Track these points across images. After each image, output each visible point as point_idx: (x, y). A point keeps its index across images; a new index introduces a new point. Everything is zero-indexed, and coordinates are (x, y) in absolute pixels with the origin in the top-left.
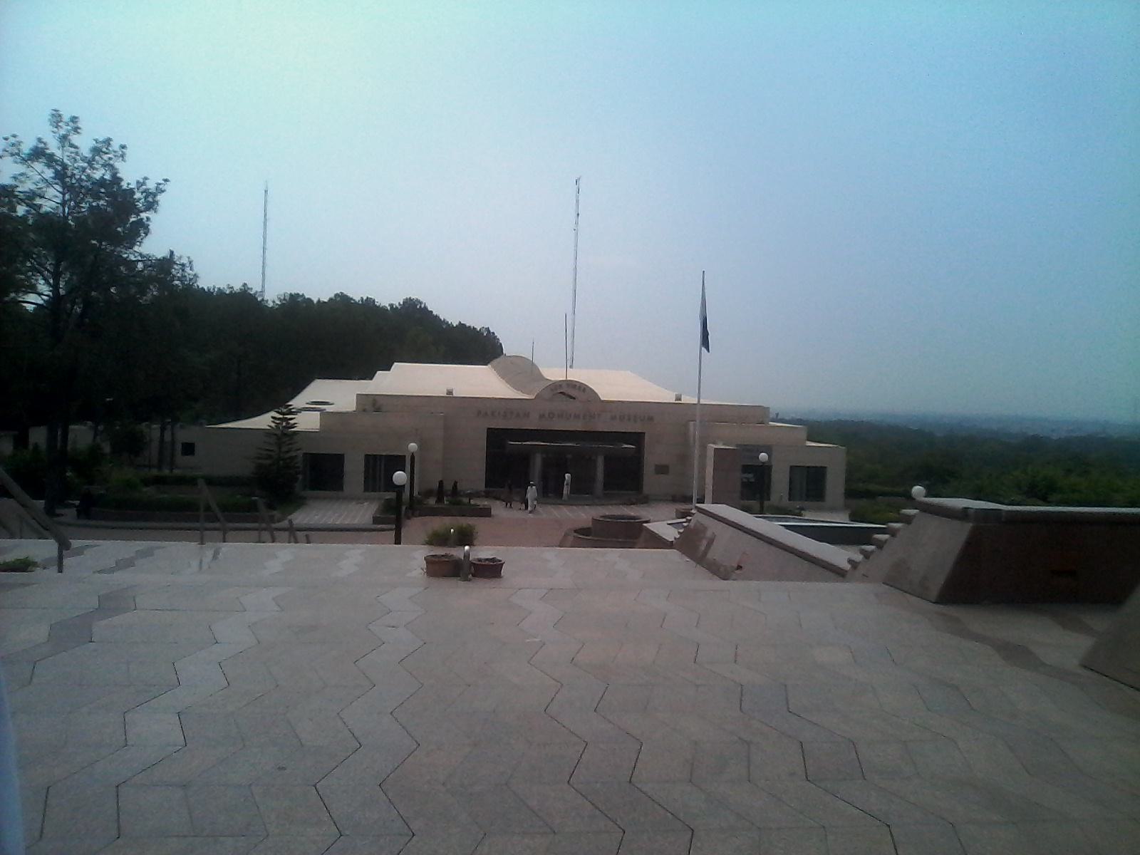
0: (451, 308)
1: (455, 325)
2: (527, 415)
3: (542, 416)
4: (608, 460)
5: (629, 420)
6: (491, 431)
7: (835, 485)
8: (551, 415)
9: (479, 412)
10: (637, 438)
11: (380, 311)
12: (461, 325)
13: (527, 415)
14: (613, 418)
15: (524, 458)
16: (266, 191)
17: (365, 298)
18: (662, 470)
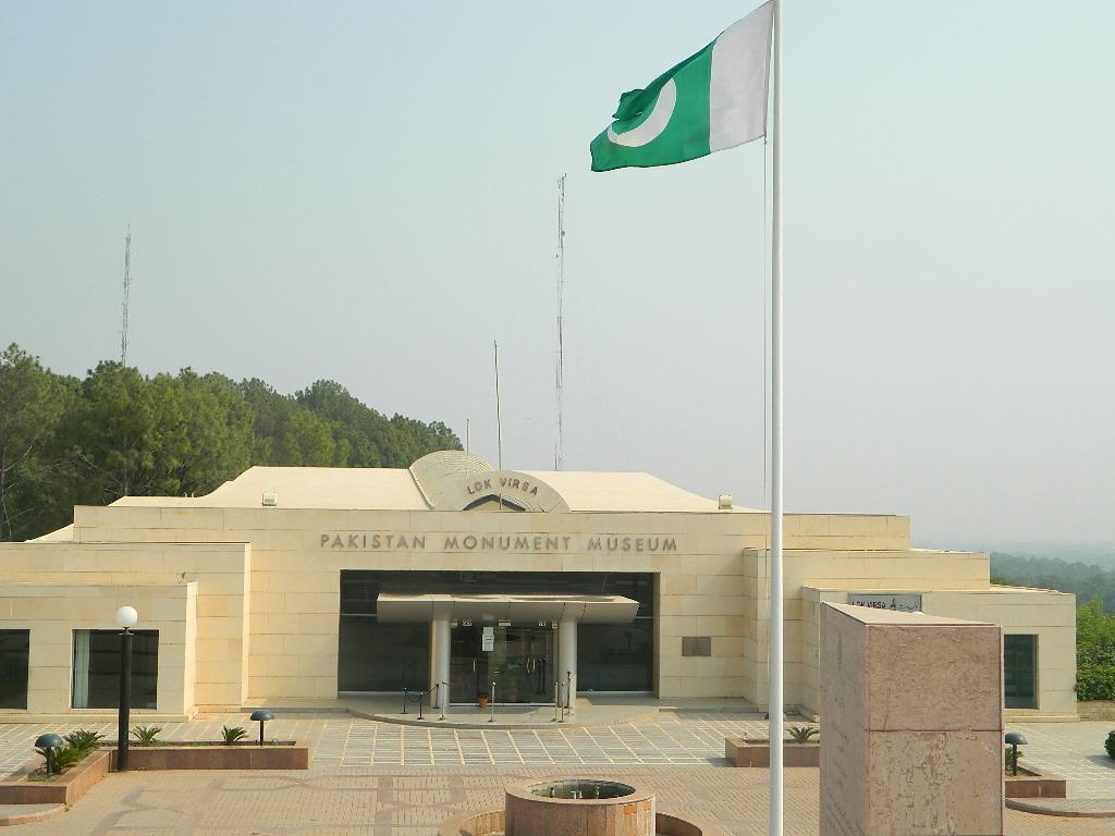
0: (383, 397)
1: (389, 419)
2: (419, 543)
3: (451, 543)
4: (589, 632)
6: (345, 575)
7: (1057, 668)
8: (470, 543)
9: (324, 539)
10: (643, 586)
12: (398, 419)
14: (594, 545)
15: (416, 633)
16: (128, 240)
17: (249, 380)
18: (695, 647)
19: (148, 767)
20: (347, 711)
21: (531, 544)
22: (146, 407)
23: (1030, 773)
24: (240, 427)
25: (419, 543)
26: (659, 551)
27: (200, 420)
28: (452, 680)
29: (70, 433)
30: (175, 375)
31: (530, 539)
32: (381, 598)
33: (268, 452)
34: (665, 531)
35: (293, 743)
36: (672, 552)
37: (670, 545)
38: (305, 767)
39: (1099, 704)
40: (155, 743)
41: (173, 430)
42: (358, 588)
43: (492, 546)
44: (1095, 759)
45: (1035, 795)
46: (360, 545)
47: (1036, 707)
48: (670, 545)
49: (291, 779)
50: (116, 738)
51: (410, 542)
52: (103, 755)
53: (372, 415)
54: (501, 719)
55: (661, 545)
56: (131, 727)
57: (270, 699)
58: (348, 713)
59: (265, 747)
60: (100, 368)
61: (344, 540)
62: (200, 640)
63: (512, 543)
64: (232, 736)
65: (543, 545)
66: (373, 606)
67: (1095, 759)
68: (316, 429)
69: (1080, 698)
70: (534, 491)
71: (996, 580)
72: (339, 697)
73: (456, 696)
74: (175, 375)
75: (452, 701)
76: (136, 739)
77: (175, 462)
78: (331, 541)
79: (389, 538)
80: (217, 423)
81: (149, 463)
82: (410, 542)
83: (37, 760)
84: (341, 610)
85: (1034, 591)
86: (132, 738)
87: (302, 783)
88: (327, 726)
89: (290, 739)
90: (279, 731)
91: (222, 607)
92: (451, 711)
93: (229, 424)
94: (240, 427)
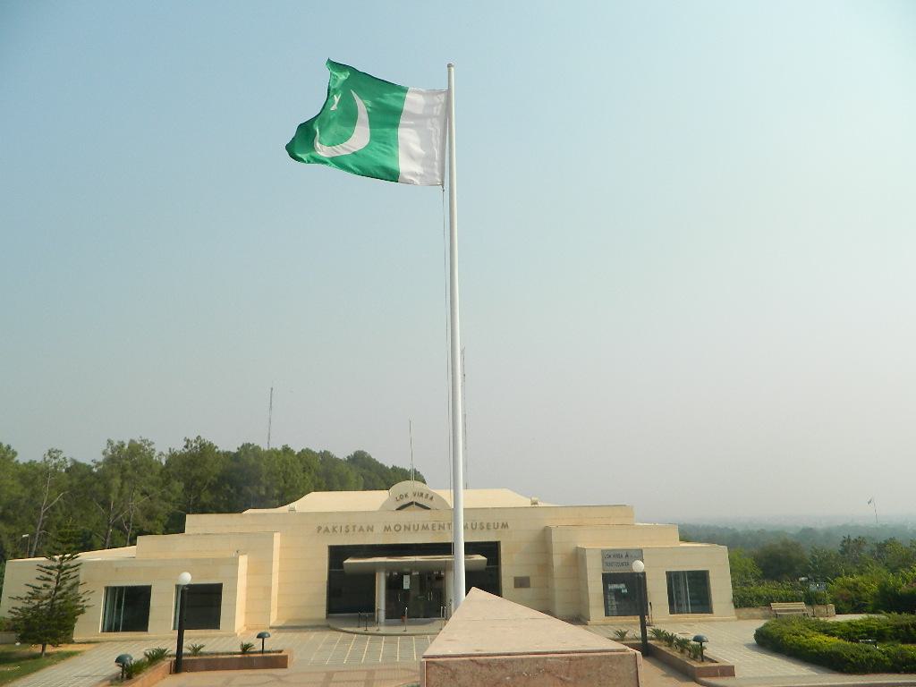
3: (387, 529)
5: (482, 528)
7: (721, 589)
8: (398, 528)
9: (319, 528)
11: (336, 461)
12: (394, 468)
13: (371, 529)
15: (368, 577)
16: (272, 389)
19: (193, 669)
20: (329, 626)
21: (430, 527)
22: (262, 464)
23: (712, 661)
24: (310, 473)
25: (371, 529)
26: (499, 529)
27: (288, 470)
28: (387, 606)
29: (224, 478)
30: (279, 448)
31: (430, 528)
32: (345, 562)
33: (324, 485)
34: (501, 517)
35: (281, 652)
36: (506, 529)
37: (505, 526)
38: (286, 667)
39: (747, 609)
40: (201, 654)
41: (275, 475)
42: (337, 554)
43: (409, 529)
44: (748, 646)
45: (716, 676)
46: (339, 532)
47: (711, 612)
48: (505, 526)
49: (272, 675)
50: (175, 651)
51: (365, 529)
52: (166, 664)
53: (382, 466)
54: (411, 629)
55: (500, 525)
56: (185, 643)
57: (290, 620)
58: (329, 628)
59: (265, 655)
60: (243, 446)
61: (330, 528)
62: (248, 588)
63: (420, 527)
64: (245, 649)
65: (437, 528)
66: (341, 566)
67: (748, 646)
68: (347, 473)
69: (736, 607)
70: (432, 498)
71: (684, 539)
72: (327, 617)
73: (389, 615)
74: (279, 448)
75: (387, 618)
76: (189, 651)
77: (276, 492)
78: (323, 529)
79: (354, 527)
80: (297, 471)
81: (264, 493)
82: (365, 529)
83: (117, 669)
84: (331, 566)
85: (703, 545)
86: (185, 650)
87: (279, 680)
88: (313, 636)
89: (279, 648)
90: (274, 643)
91: (261, 569)
92: (387, 625)
93: (304, 471)
94: (310, 473)
